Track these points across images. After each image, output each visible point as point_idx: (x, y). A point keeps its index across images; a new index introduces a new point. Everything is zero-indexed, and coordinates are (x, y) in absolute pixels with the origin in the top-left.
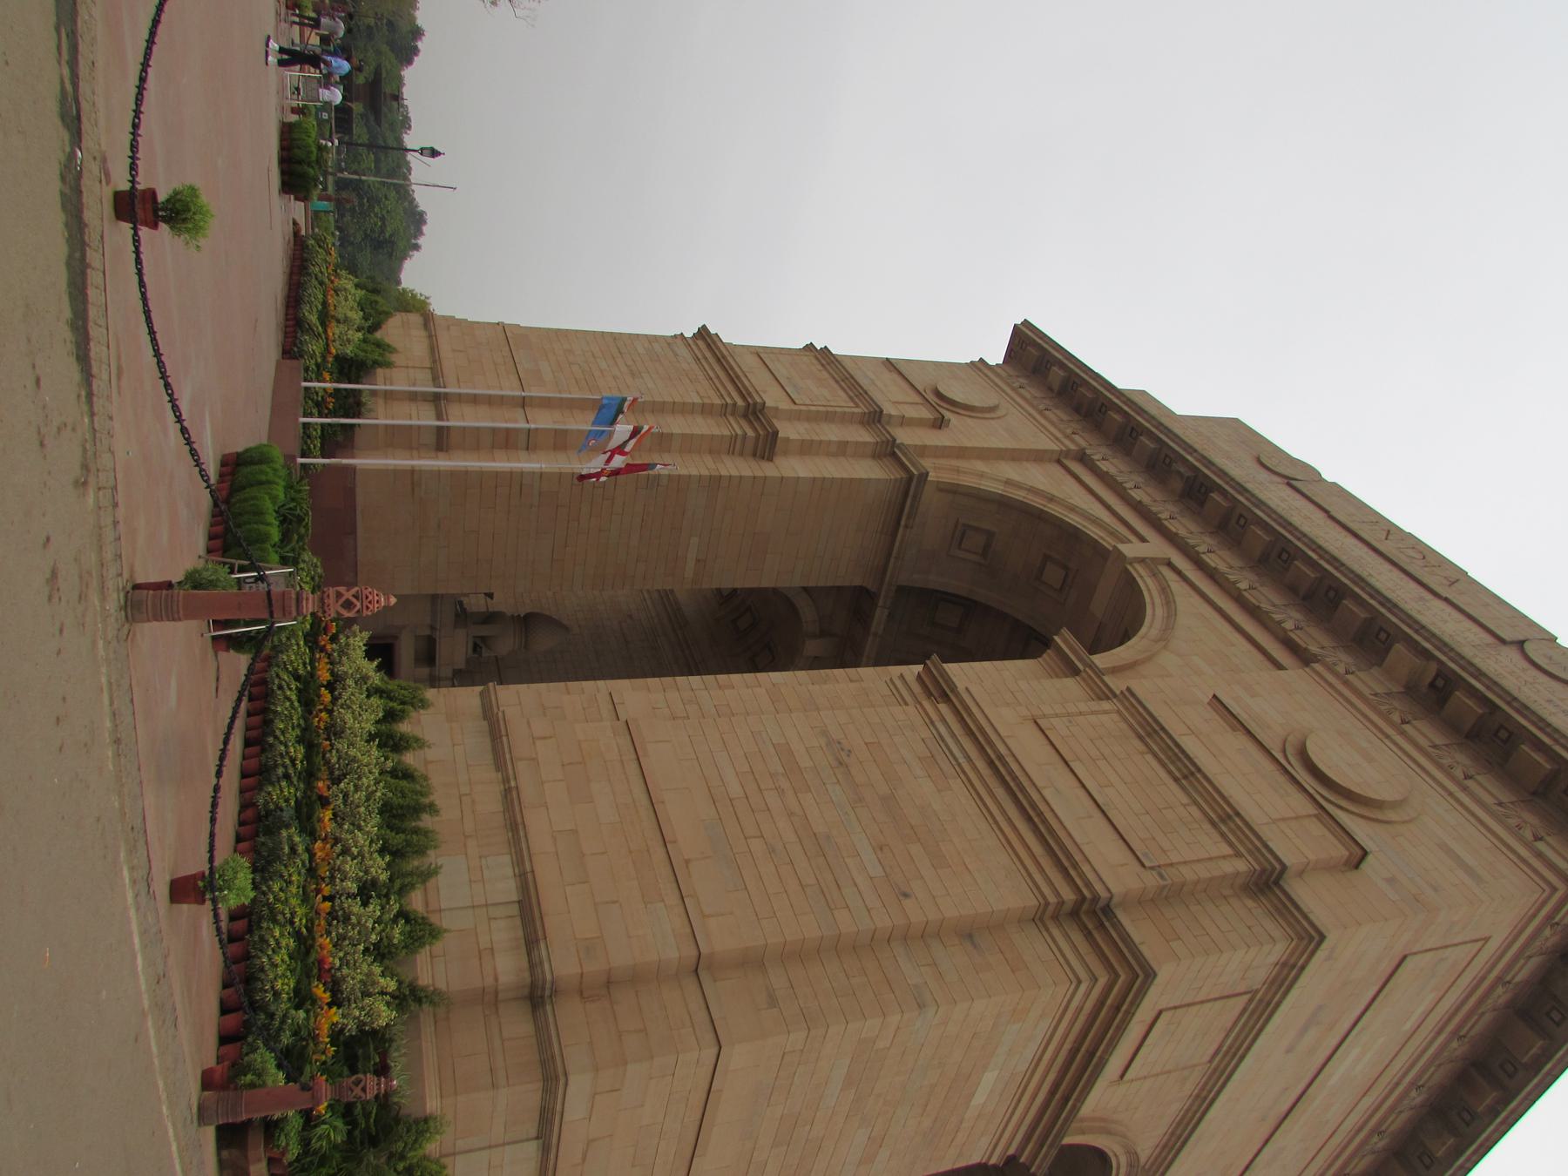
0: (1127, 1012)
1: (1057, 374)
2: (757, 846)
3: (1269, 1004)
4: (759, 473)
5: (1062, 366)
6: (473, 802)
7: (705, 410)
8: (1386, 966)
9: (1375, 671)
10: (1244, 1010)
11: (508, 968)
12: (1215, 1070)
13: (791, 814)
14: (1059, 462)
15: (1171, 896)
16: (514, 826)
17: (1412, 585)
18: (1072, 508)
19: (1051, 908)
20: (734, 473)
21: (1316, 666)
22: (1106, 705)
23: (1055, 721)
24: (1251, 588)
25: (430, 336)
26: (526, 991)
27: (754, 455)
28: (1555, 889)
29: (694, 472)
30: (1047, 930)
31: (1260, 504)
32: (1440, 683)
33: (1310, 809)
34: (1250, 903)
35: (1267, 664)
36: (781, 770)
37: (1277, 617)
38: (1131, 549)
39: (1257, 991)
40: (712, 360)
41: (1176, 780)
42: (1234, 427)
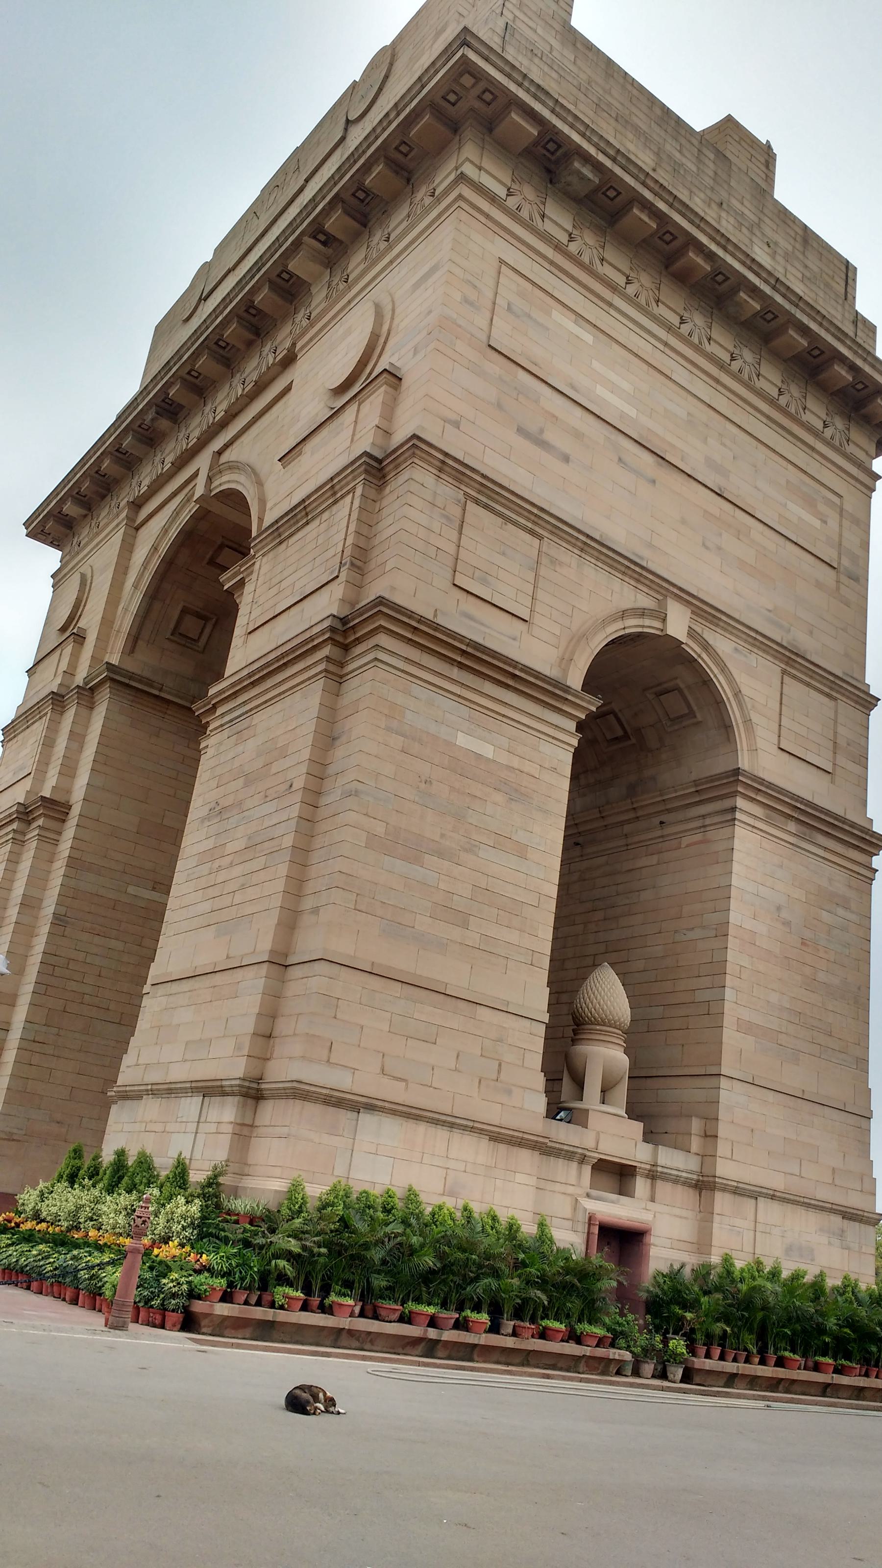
0: (419, 622)
1: (69, 508)
2: (238, 898)
3: (482, 484)
5: (62, 501)
6: (151, 1121)
7: (13, 860)
8: (495, 367)
9: (314, 290)
10: (486, 507)
12: (552, 533)
14: (137, 529)
15: (359, 560)
18: (165, 530)
19: (332, 668)
26: (250, 1102)
27: (64, 821)
28: (460, 197)
29: (59, 881)
30: (347, 674)
32: (322, 237)
33: (354, 407)
37: (264, 369)
39: (466, 494)
41: (307, 523)
42: (162, 331)
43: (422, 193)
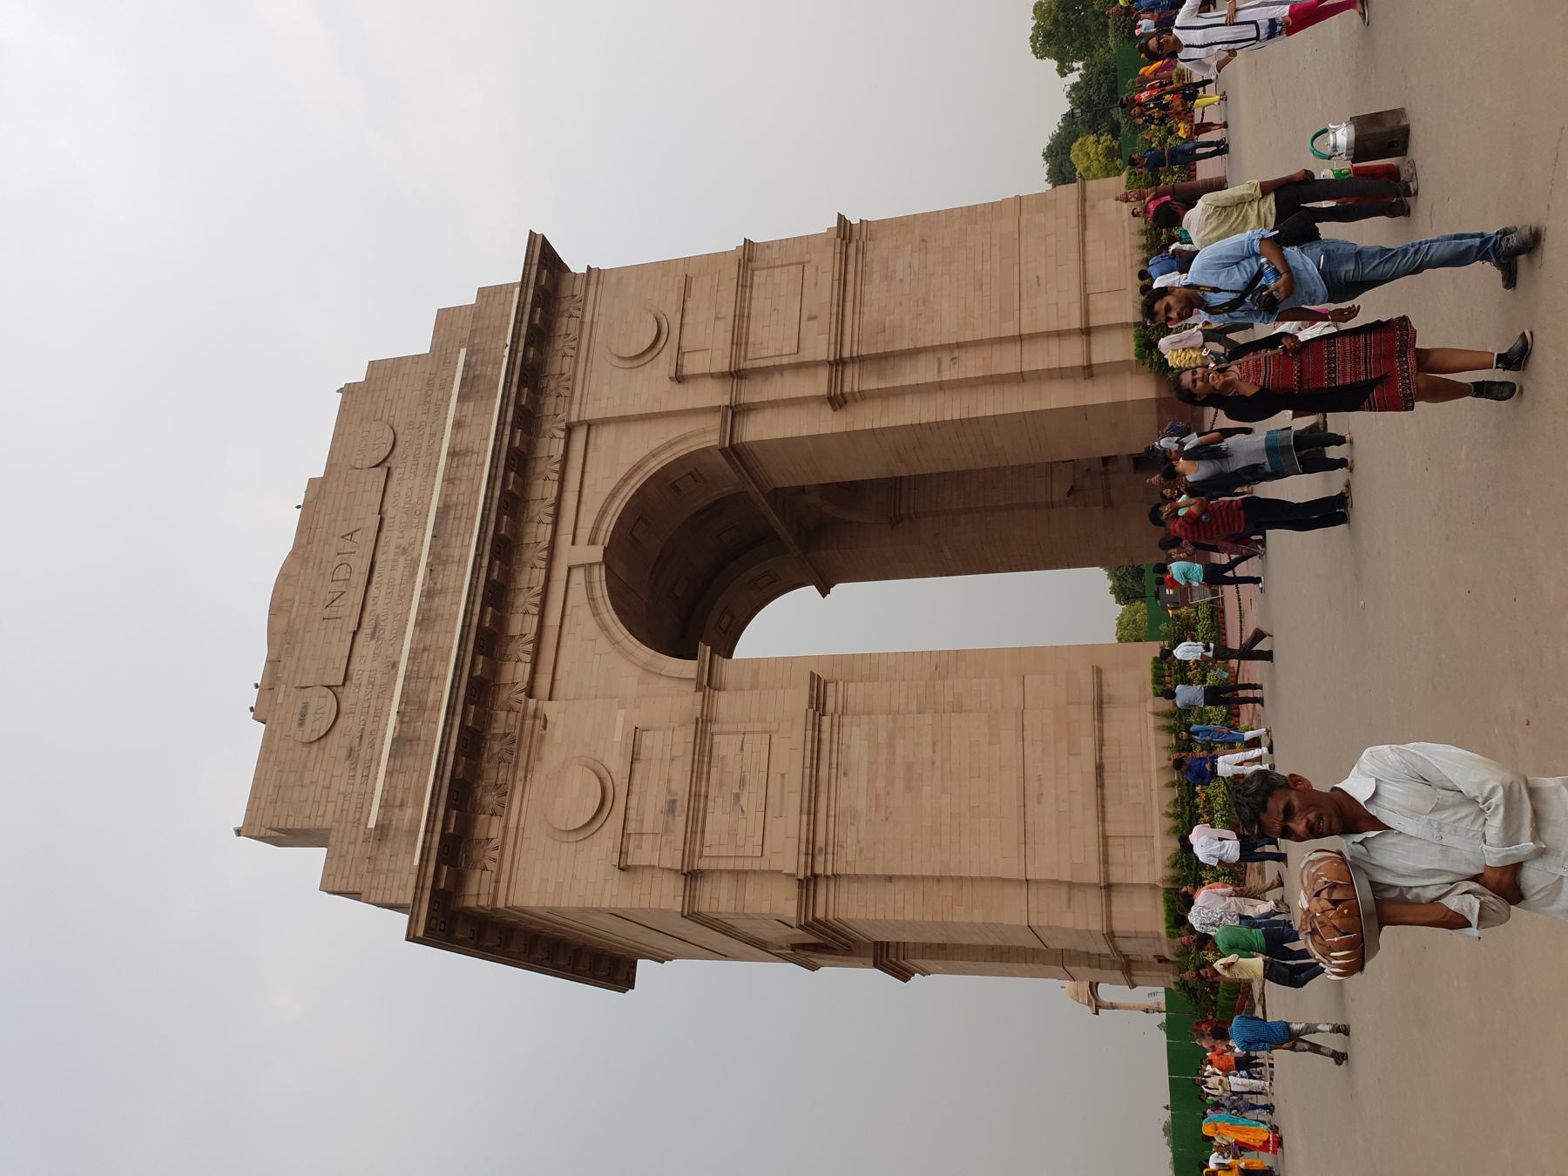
21: (574, 419)
22: (748, 365)
38: (597, 553)
43: (565, 305)
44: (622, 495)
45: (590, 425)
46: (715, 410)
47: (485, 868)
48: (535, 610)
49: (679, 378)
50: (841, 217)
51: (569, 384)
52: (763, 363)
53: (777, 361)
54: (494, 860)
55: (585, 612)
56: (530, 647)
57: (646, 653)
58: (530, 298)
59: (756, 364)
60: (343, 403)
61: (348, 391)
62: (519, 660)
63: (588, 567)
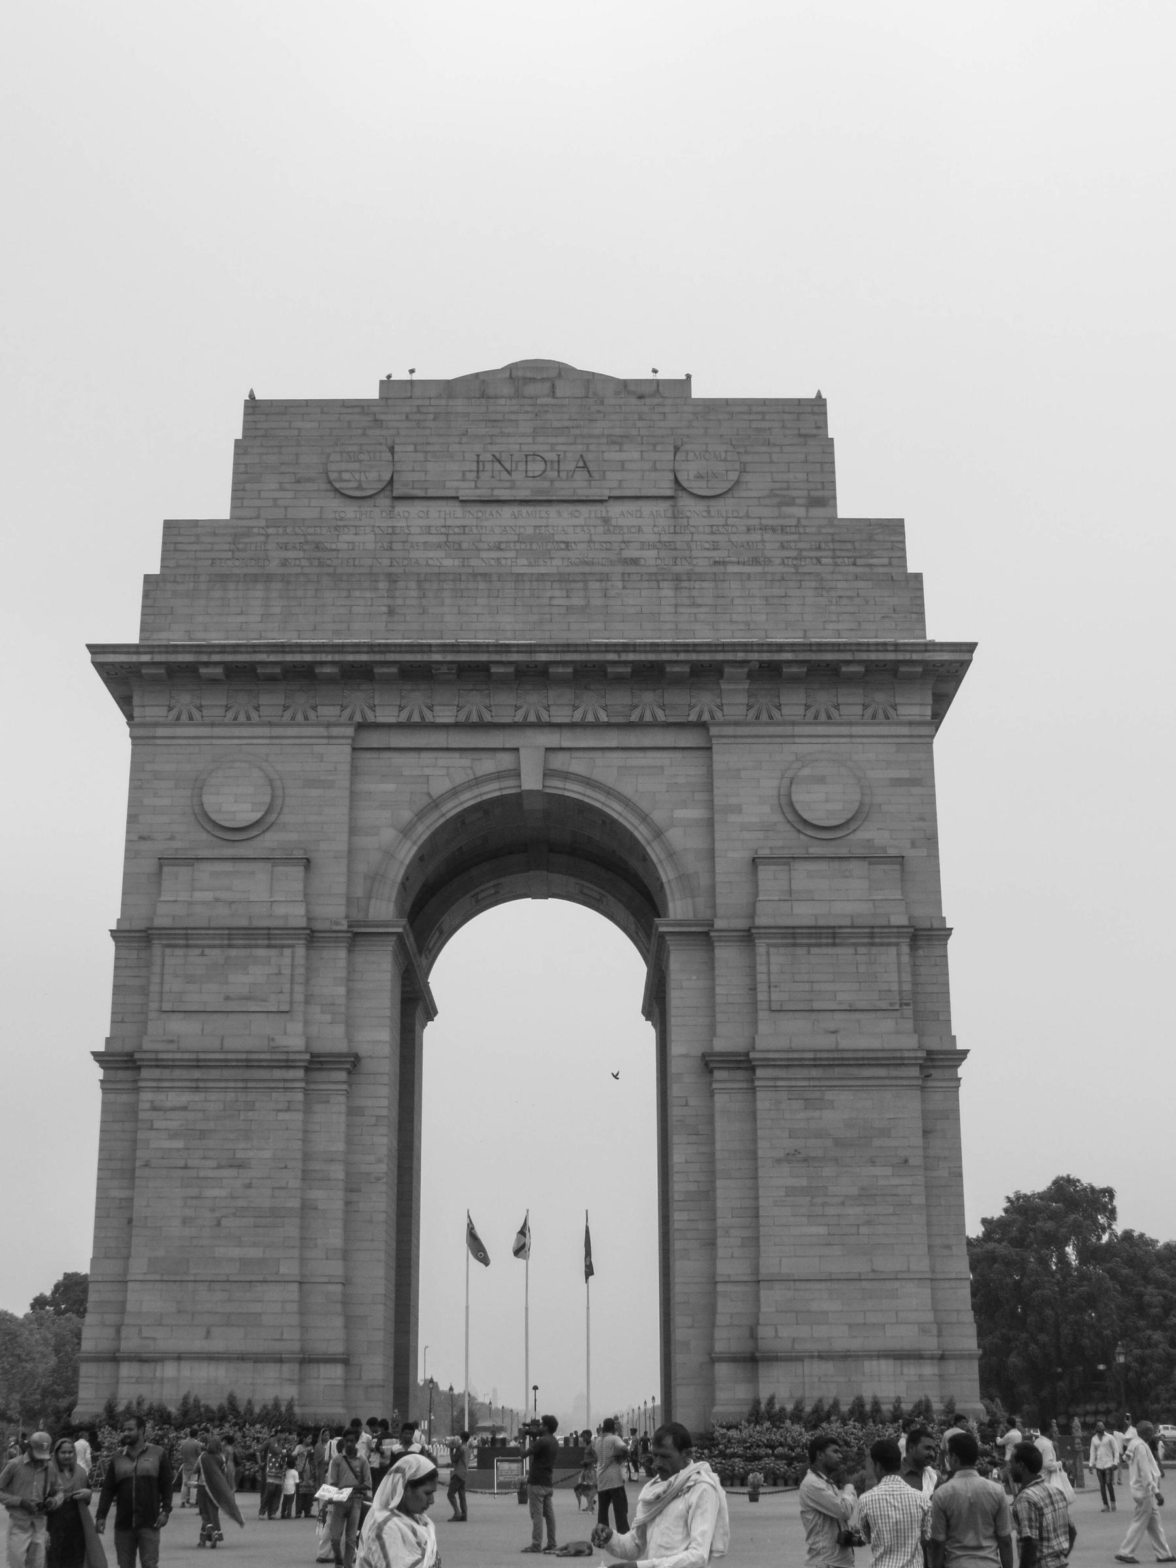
4: (386, 1079)
5: (207, 664)
7: (307, 1110)
11: (929, 1369)
13: (843, 1204)
16: (845, 1356)
17: (584, 510)
18: (455, 792)
20: (385, 1103)
21: (714, 731)
22: (761, 949)
23: (774, 997)
24: (605, 708)
25: (179, 1358)
31: (530, 649)
34: (920, 952)
35: (687, 754)
36: (809, 1198)
38: (531, 781)
40: (197, 1074)
41: (834, 945)
43: (881, 698)
44: (608, 802)
45: (710, 749)
46: (714, 906)
47: (170, 708)
48: (462, 718)
49: (755, 862)
50: (965, 1053)
51: (764, 717)
52: (761, 968)
53: (762, 987)
54: (178, 718)
55: (461, 778)
56: (416, 718)
57: (407, 852)
58: (873, 656)
59: (761, 959)
60: (799, 402)
61: (818, 406)
62: (401, 708)
63: (516, 774)
